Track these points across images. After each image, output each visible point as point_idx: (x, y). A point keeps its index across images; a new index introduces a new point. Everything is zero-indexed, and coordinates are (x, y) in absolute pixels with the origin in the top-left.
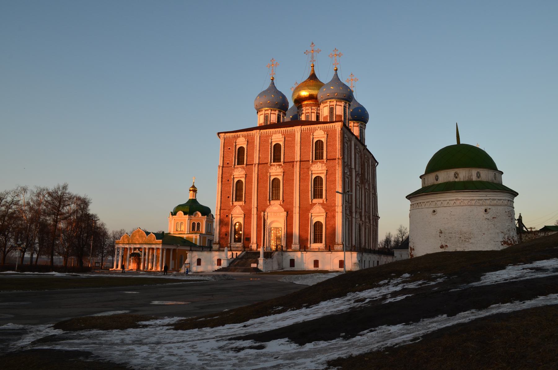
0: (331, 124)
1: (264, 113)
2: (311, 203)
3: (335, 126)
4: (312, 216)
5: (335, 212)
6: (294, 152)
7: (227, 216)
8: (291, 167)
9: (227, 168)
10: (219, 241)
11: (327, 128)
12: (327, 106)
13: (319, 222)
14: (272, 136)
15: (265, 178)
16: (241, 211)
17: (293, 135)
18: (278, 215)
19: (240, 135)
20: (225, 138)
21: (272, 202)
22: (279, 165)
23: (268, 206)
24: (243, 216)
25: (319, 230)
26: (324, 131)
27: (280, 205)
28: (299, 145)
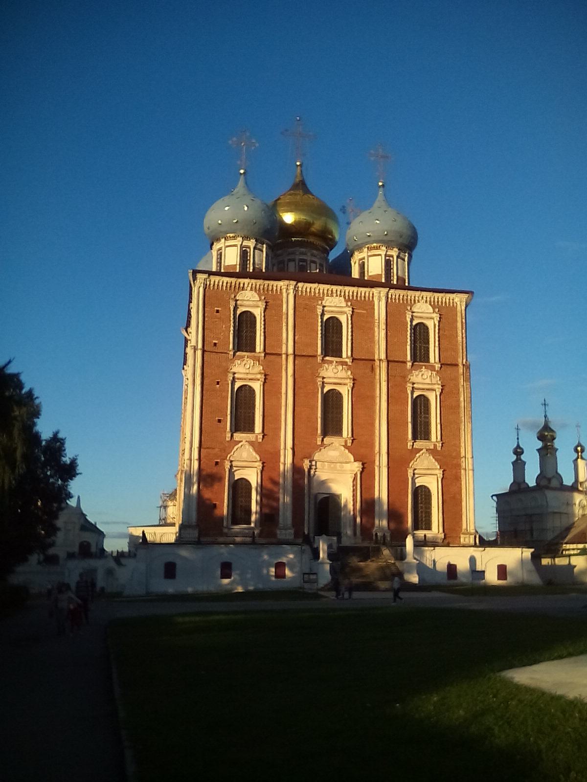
0: (449, 296)
1: (239, 244)
2: (409, 447)
3: (455, 301)
4: (414, 474)
5: (460, 469)
6: (371, 339)
7: (217, 463)
8: (368, 371)
9: (213, 355)
10: (198, 519)
11: (438, 302)
12: (380, 255)
13: (425, 487)
14: (322, 299)
15: (311, 388)
16: (254, 454)
17: (369, 305)
18: (338, 468)
19: (246, 285)
20: (206, 285)
21: (327, 440)
22: (344, 363)
23: (319, 448)
24: (259, 465)
25: (421, 503)
26: (434, 307)
27: (346, 446)
28: (383, 326)
